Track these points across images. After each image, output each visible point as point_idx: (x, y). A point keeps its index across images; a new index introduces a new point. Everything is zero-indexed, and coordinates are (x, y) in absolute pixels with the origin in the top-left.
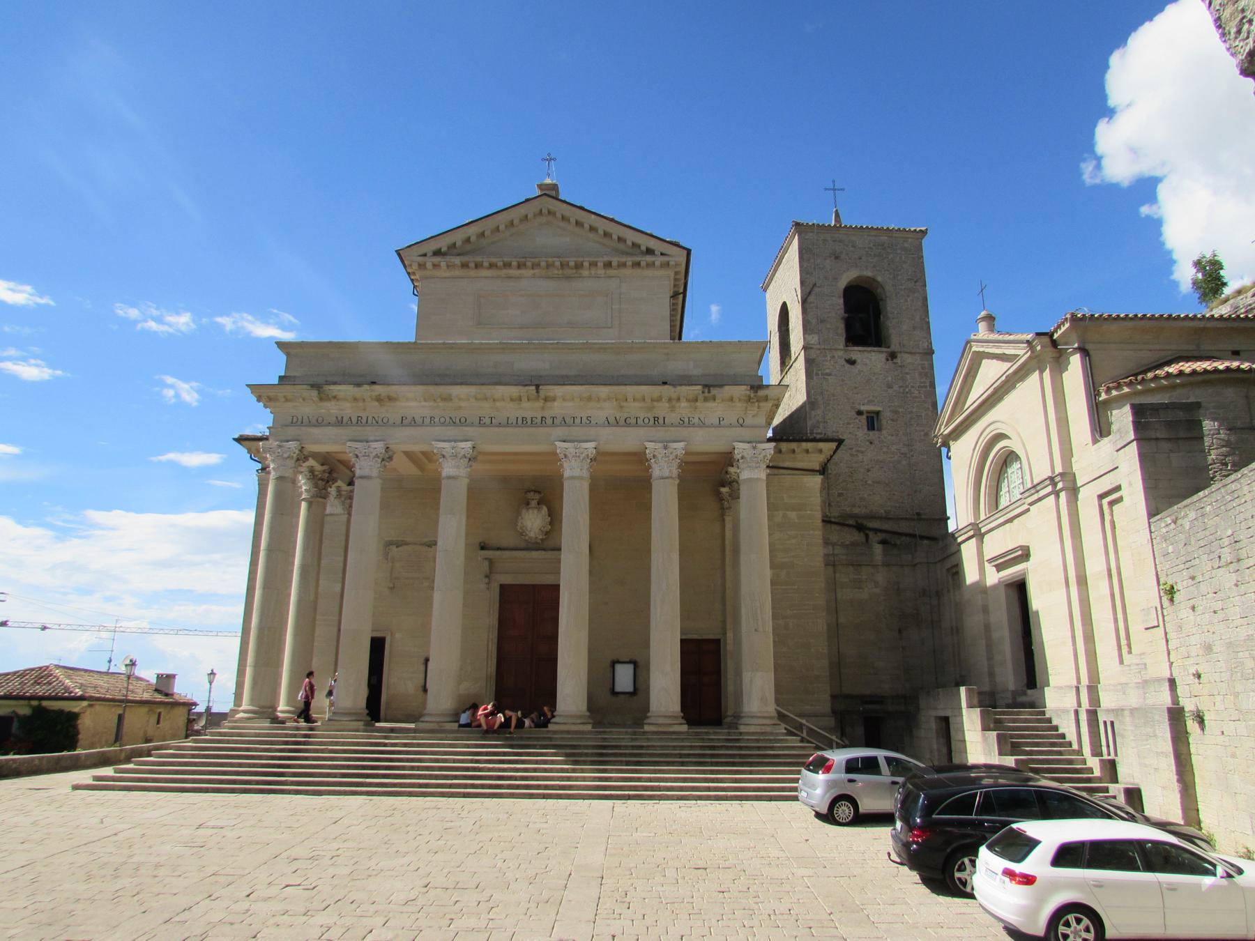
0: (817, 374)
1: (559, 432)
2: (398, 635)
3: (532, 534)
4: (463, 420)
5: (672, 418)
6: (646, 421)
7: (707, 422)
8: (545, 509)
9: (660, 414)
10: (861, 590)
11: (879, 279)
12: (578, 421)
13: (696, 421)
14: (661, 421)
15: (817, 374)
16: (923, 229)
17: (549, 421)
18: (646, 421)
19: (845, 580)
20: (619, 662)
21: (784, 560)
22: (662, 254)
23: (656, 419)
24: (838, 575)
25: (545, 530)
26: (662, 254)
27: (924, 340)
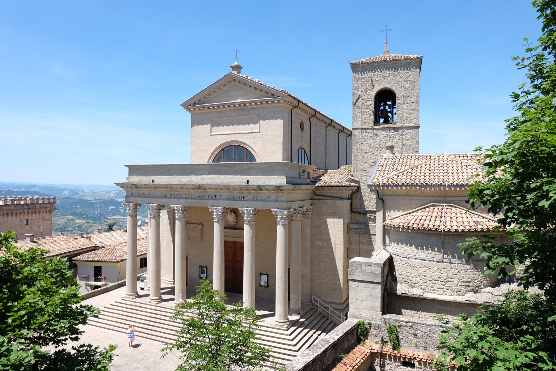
0: (358, 142)
1: (210, 202)
2: (191, 256)
3: (231, 223)
4: (180, 196)
5: (250, 197)
6: (241, 197)
7: (263, 199)
8: (233, 214)
9: (246, 195)
10: (371, 245)
11: (393, 88)
12: (217, 197)
13: (259, 198)
14: (246, 198)
15: (358, 142)
16: (419, 56)
17: (207, 197)
18: (241, 197)
19: (364, 240)
20: (262, 274)
21: (326, 238)
22: (278, 97)
23: (244, 197)
24: (361, 238)
25: (234, 221)
26: (278, 97)
27: (416, 119)
